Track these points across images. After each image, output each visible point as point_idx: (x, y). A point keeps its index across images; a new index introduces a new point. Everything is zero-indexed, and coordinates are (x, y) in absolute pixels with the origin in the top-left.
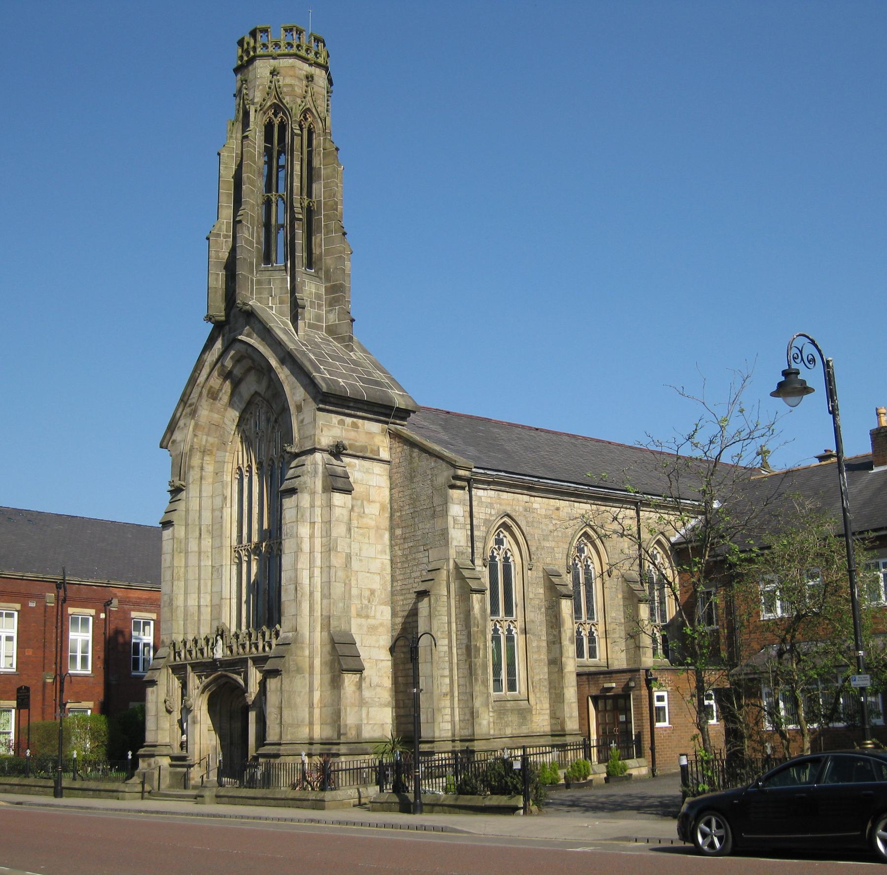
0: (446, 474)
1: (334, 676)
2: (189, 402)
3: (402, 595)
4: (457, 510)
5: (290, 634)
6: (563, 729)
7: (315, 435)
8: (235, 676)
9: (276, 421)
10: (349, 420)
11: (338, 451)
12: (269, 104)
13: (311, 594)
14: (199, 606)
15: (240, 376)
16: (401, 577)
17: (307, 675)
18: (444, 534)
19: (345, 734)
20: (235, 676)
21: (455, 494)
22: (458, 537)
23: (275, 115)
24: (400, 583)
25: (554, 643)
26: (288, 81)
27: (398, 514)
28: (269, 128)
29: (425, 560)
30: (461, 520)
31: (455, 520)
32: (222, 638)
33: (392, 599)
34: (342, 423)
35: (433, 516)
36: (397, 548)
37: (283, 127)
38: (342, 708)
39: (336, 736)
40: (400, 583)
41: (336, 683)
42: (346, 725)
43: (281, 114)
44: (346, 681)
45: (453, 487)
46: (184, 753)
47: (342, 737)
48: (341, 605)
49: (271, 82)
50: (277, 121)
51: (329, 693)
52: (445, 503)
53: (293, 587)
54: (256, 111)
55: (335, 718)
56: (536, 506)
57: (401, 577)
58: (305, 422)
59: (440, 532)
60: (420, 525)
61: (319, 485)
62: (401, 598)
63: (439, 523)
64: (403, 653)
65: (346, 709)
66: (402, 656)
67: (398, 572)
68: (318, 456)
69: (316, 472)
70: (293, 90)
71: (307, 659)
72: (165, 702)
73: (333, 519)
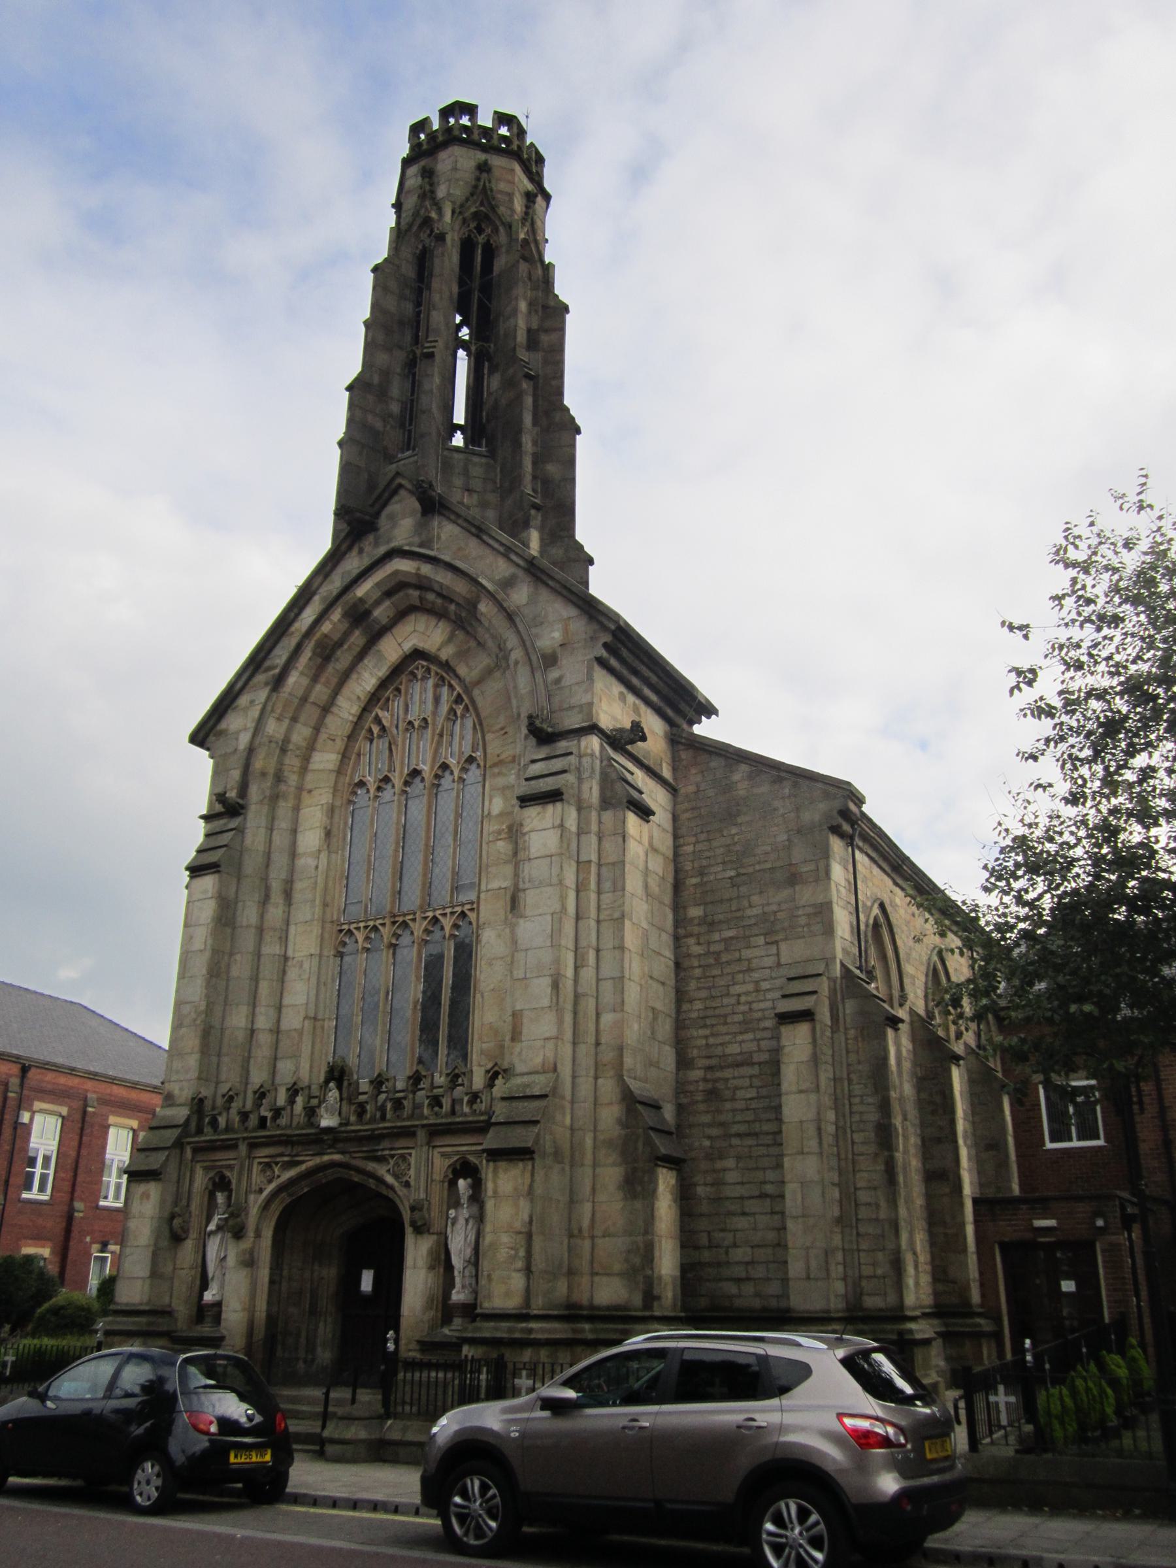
0: (823, 806)
1: (634, 1170)
2: (267, 663)
3: (705, 1026)
4: (838, 873)
5: (541, 1079)
6: (901, 1306)
7: (591, 704)
8: (371, 1166)
9: (459, 700)
10: (631, 698)
11: (622, 740)
12: (473, 210)
13: (577, 996)
14: (253, 1031)
15: (384, 621)
16: (704, 994)
17: (567, 1168)
18: (823, 911)
19: (658, 1298)
20: (371, 1166)
21: (837, 845)
22: (842, 919)
23: (480, 230)
24: (698, 1005)
25: (939, 1140)
26: (502, 186)
27: (694, 881)
28: (467, 247)
29: (769, 961)
30: (843, 891)
31: (838, 891)
32: (340, 1087)
33: (677, 1035)
34: (622, 698)
35: (794, 880)
36: (691, 941)
37: (490, 252)
38: (656, 1239)
39: (637, 1300)
40: (698, 1005)
41: (637, 1186)
42: (660, 1278)
43: (489, 231)
44: (661, 1181)
45: (836, 830)
46: (206, 1330)
47: (656, 1304)
48: (636, 1026)
49: (478, 179)
50: (481, 239)
51: (620, 1205)
52: (826, 855)
53: (546, 982)
54: (453, 212)
55: (637, 1261)
56: (898, 901)
57: (704, 994)
58: (566, 682)
59: (810, 910)
60: (755, 899)
61: (592, 791)
62: (702, 1032)
63: (806, 895)
64: (709, 1137)
65: (660, 1242)
66: (707, 1143)
67: (693, 985)
68: (594, 743)
69: (593, 771)
70: (511, 201)
71: (568, 1134)
72: (172, 1217)
73: (628, 859)
